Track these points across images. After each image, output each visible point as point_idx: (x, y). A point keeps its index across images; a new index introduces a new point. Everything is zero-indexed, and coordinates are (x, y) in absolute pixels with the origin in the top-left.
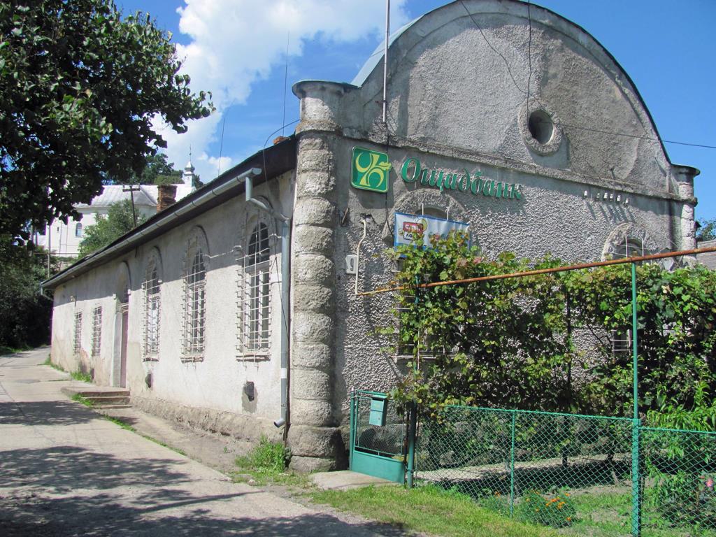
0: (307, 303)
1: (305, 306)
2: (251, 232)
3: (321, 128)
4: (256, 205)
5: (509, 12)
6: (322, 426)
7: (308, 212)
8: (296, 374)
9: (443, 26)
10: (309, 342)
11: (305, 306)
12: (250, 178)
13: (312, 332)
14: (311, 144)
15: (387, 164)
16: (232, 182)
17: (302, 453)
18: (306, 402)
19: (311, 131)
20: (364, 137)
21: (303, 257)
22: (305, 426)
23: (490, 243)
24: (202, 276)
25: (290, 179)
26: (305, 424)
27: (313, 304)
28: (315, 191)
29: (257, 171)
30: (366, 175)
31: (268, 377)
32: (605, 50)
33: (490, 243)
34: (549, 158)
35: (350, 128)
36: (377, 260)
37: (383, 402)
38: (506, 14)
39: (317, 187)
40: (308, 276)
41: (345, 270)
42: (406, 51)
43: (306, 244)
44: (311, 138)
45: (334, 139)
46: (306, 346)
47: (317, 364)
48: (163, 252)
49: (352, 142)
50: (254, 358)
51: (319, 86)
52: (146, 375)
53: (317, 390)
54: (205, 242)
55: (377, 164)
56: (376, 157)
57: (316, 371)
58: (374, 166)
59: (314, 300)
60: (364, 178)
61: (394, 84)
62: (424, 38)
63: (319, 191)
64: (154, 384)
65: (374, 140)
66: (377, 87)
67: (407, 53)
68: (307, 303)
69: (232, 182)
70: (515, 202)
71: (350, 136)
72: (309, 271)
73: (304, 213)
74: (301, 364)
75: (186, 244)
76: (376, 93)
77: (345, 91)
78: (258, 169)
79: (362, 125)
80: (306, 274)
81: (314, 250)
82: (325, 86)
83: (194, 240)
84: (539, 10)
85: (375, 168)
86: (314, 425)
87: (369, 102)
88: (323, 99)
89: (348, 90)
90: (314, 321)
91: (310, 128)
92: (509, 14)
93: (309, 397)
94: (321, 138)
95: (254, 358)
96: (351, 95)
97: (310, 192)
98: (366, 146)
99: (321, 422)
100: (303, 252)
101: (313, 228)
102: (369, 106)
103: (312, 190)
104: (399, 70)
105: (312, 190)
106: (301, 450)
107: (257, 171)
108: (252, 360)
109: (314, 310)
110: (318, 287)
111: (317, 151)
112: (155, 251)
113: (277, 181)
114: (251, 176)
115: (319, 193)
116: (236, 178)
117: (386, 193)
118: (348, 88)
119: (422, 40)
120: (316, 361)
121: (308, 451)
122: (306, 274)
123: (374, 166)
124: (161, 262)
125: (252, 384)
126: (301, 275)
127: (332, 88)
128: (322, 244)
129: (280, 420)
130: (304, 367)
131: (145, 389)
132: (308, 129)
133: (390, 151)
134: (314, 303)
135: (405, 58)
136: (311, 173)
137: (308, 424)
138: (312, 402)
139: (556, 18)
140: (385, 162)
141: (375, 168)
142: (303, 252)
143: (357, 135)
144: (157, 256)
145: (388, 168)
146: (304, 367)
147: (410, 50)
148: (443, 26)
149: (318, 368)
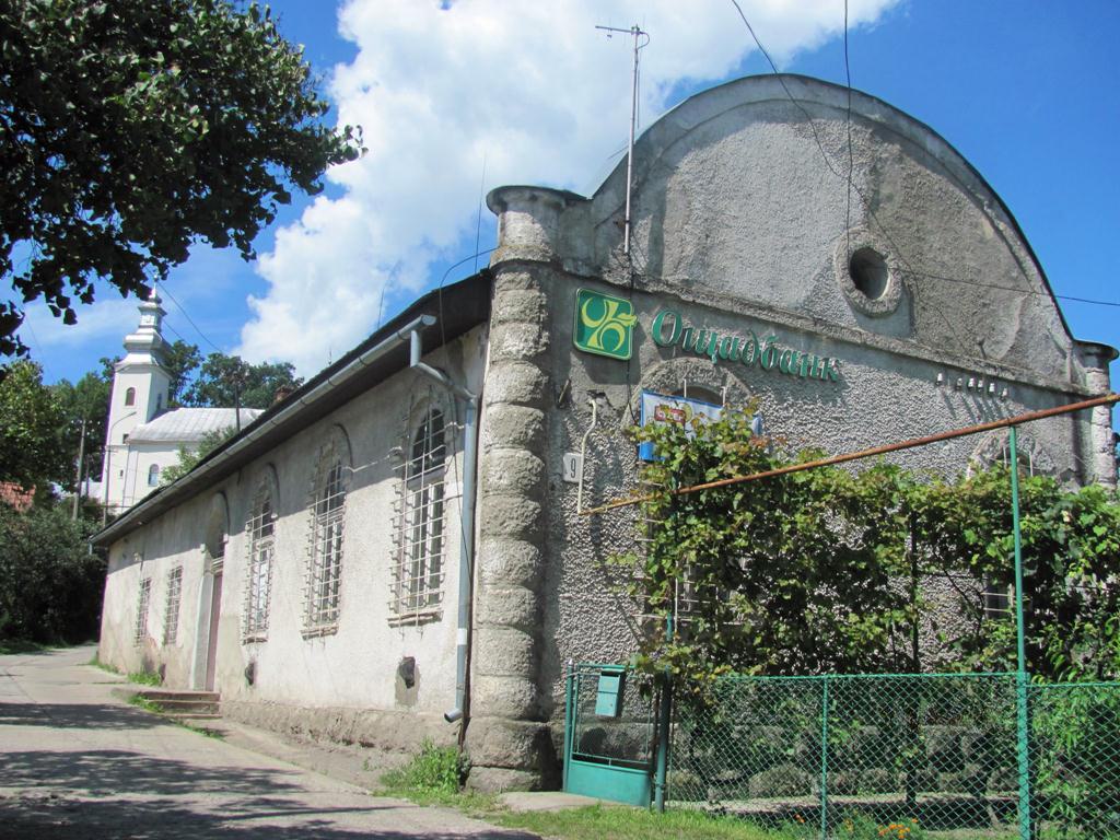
0: (502, 524)
1: (499, 529)
2: (417, 425)
3: (530, 257)
4: (425, 372)
5: (818, 100)
6: (521, 718)
7: (507, 384)
8: (482, 637)
9: (718, 116)
10: (503, 584)
11: (499, 529)
12: (418, 332)
13: (508, 568)
14: (513, 281)
15: (629, 317)
16: (392, 340)
17: (488, 761)
18: (496, 679)
19: (514, 260)
20: (595, 275)
21: (497, 453)
22: (495, 718)
23: (790, 447)
24: (339, 502)
25: (479, 338)
26: (493, 714)
27: (511, 526)
28: (518, 351)
29: (430, 320)
30: (596, 333)
31: (435, 650)
32: (966, 163)
33: (790, 447)
34: (882, 321)
35: (574, 260)
36: (612, 464)
37: (618, 679)
38: (815, 103)
39: (522, 345)
40: (504, 482)
41: (561, 475)
42: (661, 150)
43: (502, 433)
44: (514, 272)
45: (549, 275)
46: (498, 591)
47: (515, 620)
48: (281, 473)
49: (577, 282)
50: (416, 619)
51: (527, 194)
52: (247, 665)
53: (514, 661)
54: (346, 448)
55: (615, 316)
56: (614, 306)
57: (513, 630)
58: (609, 318)
59: (513, 518)
60: (595, 336)
61: (642, 196)
62: (689, 132)
63: (524, 352)
64: (260, 678)
65: (611, 280)
66: (616, 201)
67: (663, 154)
68: (502, 524)
69: (392, 340)
70: (828, 385)
71: (573, 271)
72: (506, 474)
73: (500, 386)
74: (490, 619)
75: (317, 453)
76: (616, 208)
77: (568, 204)
78: (431, 317)
79: (592, 255)
80: (500, 478)
81: (514, 442)
82: (536, 193)
83: (330, 446)
84: (864, 98)
85: (611, 322)
86: (509, 717)
87: (605, 222)
88: (533, 213)
89: (573, 202)
90: (512, 552)
91: (512, 257)
92: (820, 104)
93: (501, 672)
94: (530, 272)
95: (416, 619)
96: (578, 211)
97: (510, 353)
98: (598, 288)
99: (520, 712)
100: (497, 446)
101: (514, 408)
102: (604, 227)
103: (514, 350)
104: (650, 177)
105: (514, 350)
106: (486, 757)
107: (430, 320)
108: (412, 624)
109: (512, 534)
110: (520, 500)
111: (522, 292)
112: (269, 469)
113: (460, 342)
114: (419, 328)
115: (525, 355)
116: (396, 334)
117: (628, 361)
118: (570, 198)
119: (686, 135)
120: (514, 615)
121: (497, 759)
122: (500, 478)
123: (609, 318)
124: (278, 487)
125: (412, 660)
126: (493, 480)
127: (546, 197)
128: (526, 434)
129: (455, 710)
130: (493, 624)
131: (243, 688)
132: (508, 258)
133: (636, 298)
134: (513, 523)
135: (660, 159)
136: (513, 325)
137: (498, 715)
139: (891, 112)
140: (628, 313)
141: (611, 322)
142: (497, 446)
143: (584, 271)
144: (271, 479)
145: (632, 323)
146: (493, 624)
147: (668, 149)
148: (718, 116)
149: (517, 626)
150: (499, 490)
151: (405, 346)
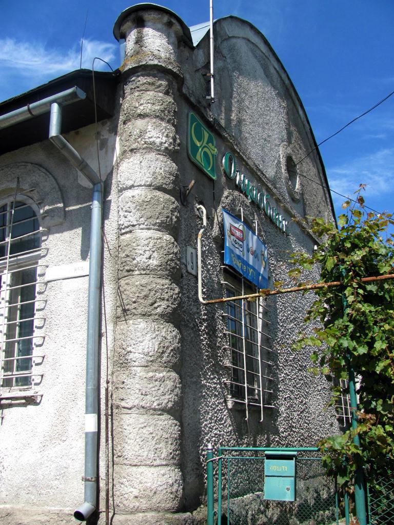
0: (152, 304)
1: (149, 309)
6: (178, 511)
7: (152, 170)
10: (156, 366)
11: (149, 309)
12: (59, 104)
13: (161, 350)
14: (153, 84)
18: (153, 470)
19: (155, 66)
22: (153, 514)
26: (151, 510)
28: (161, 143)
37: (293, 462)
39: (164, 139)
40: (154, 262)
43: (149, 214)
44: (154, 76)
46: (151, 374)
47: (170, 405)
53: (170, 448)
57: (166, 416)
59: (163, 300)
63: (166, 145)
68: (152, 304)
72: (155, 254)
73: (145, 170)
74: (143, 403)
80: (150, 258)
81: (160, 225)
86: (168, 510)
88: (168, 36)
90: (163, 334)
91: (156, 62)
93: (158, 462)
94: (168, 80)
99: (175, 503)
100: (142, 226)
103: (158, 141)
105: (158, 141)
109: (162, 316)
110: (167, 281)
111: (161, 94)
114: (60, 102)
115: (166, 148)
116: (25, 108)
120: (168, 400)
122: (150, 258)
128: (171, 219)
130: (146, 410)
132: (152, 63)
134: (164, 304)
136: (154, 120)
137: (157, 510)
138: (163, 470)
142: (142, 226)
146: (146, 410)
149: (164, 410)
150: (147, 270)
151: (45, 117)
